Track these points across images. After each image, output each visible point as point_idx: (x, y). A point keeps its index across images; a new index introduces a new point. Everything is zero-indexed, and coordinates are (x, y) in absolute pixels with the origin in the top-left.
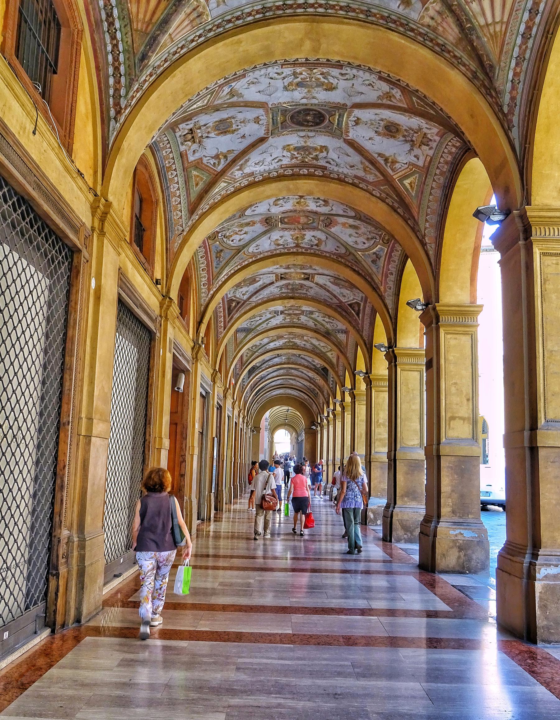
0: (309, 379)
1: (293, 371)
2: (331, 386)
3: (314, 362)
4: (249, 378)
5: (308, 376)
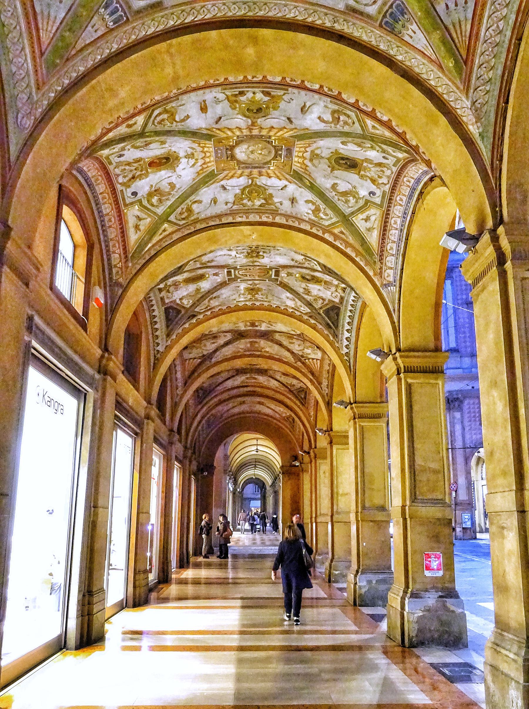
0: (291, 359)
1: (262, 343)
2: (345, 350)
3: (308, 292)
4: (168, 335)
5: (292, 353)
